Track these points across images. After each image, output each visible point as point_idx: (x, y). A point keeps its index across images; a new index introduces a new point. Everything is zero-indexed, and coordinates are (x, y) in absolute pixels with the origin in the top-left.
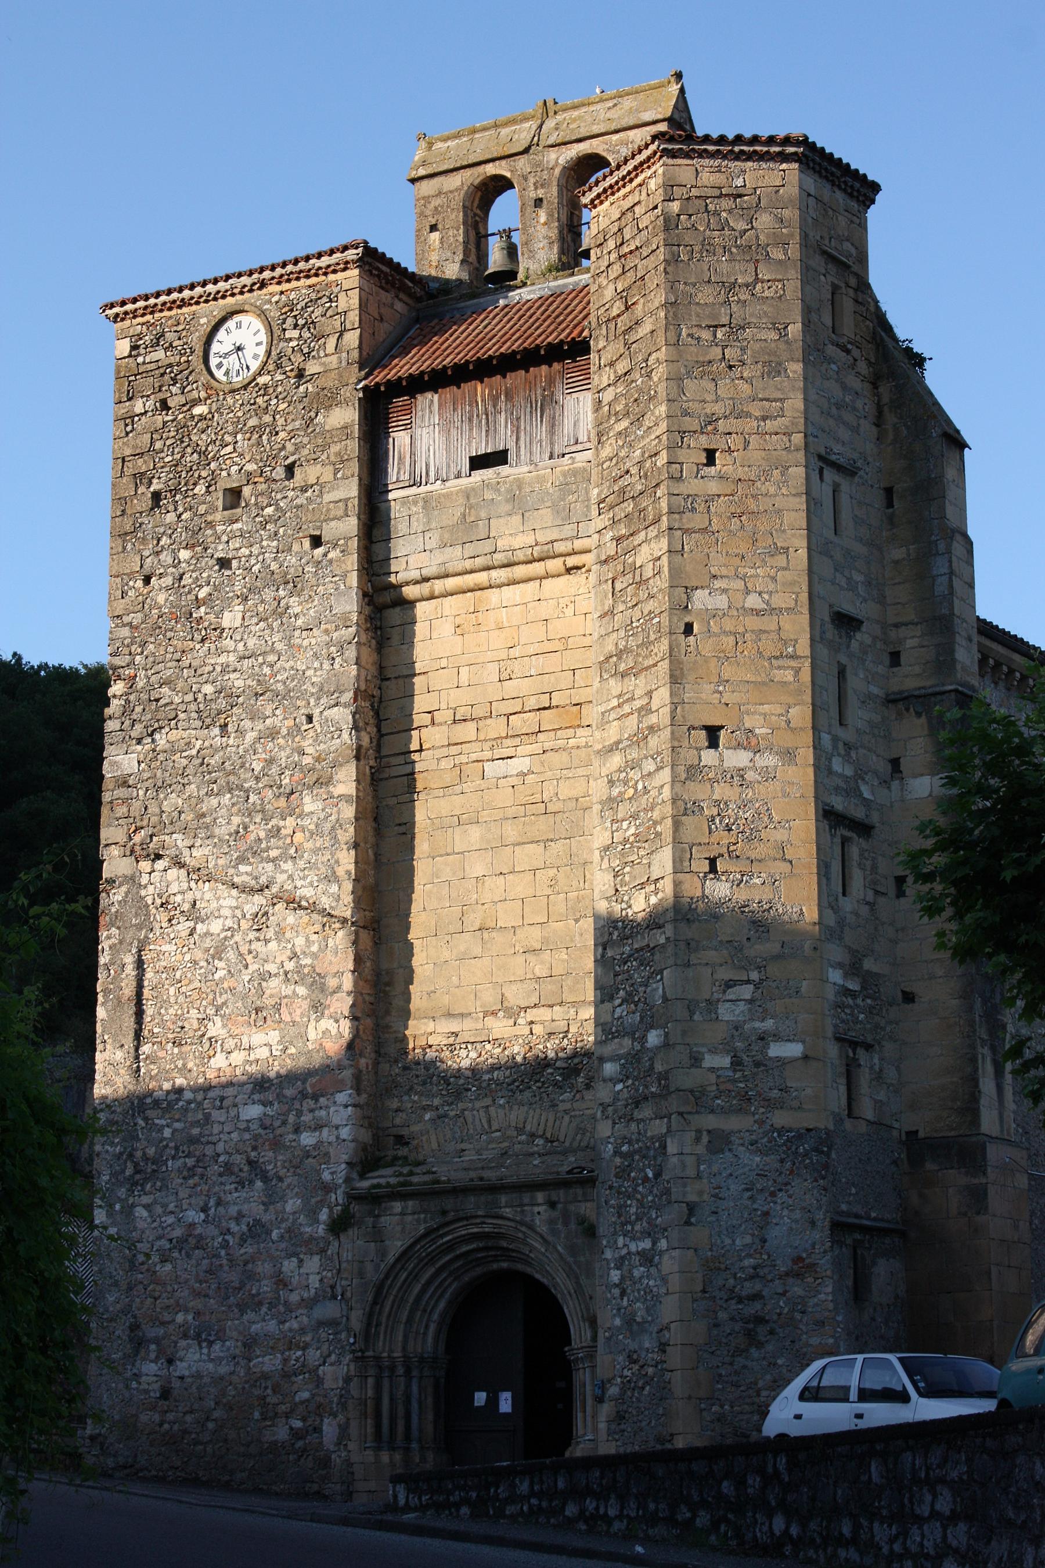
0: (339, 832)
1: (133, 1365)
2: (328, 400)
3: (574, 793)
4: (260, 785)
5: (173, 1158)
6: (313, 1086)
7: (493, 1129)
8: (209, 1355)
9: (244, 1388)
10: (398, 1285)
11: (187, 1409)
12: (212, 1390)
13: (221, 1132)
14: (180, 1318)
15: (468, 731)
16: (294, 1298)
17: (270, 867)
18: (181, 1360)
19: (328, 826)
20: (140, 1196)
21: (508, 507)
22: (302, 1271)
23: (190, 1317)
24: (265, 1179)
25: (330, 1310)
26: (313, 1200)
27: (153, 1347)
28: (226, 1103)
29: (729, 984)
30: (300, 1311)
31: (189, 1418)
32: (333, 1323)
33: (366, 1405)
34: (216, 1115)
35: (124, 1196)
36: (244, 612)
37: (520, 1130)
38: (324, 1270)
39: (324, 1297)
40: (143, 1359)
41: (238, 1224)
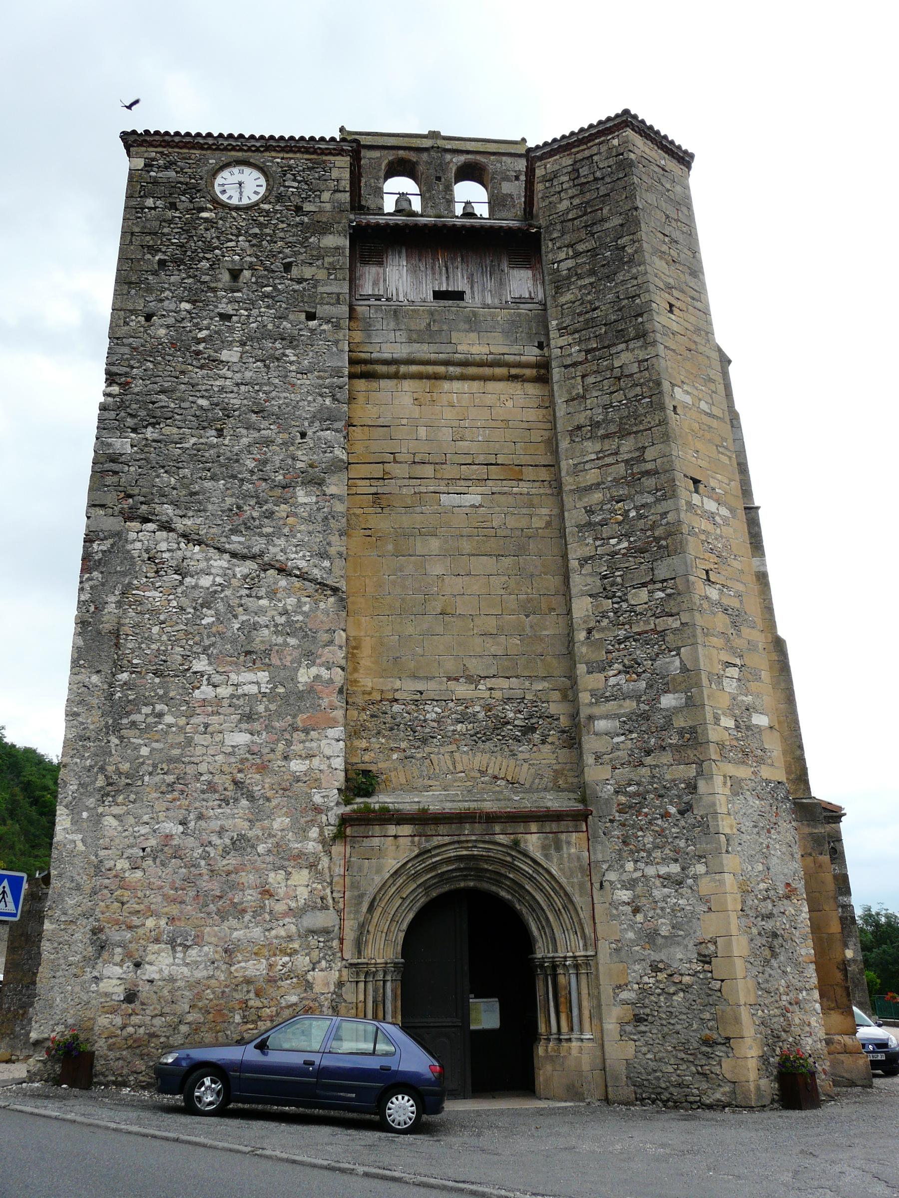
0: (332, 521)
1: (93, 968)
2: (323, 229)
3: (520, 525)
4: (254, 477)
5: (150, 774)
6: (303, 721)
7: (458, 770)
8: (183, 959)
9: (223, 992)
10: (387, 898)
11: (157, 1012)
12: (187, 993)
13: (204, 755)
14: (150, 923)
15: (428, 471)
16: (280, 907)
17: (263, 541)
18: (151, 964)
19: (320, 516)
20: (110, 806)
21: (467, 326)
22: (289, 882)
23: (163, 922)
24: (251, 798)
25: (326, 919)
26: (303, 820)
27: (119, 950)
28: (210, 729)
29: (729, 664)
30: (287, 920)
31: (158, 1021)
32: (326, 931)
34: (198, 739)
35: (92, 806)
36: (243, 353)
37: (483, 773)
38: (314, 882)
39: (314, 908)
40: (105, 962)
41: (221, 838)
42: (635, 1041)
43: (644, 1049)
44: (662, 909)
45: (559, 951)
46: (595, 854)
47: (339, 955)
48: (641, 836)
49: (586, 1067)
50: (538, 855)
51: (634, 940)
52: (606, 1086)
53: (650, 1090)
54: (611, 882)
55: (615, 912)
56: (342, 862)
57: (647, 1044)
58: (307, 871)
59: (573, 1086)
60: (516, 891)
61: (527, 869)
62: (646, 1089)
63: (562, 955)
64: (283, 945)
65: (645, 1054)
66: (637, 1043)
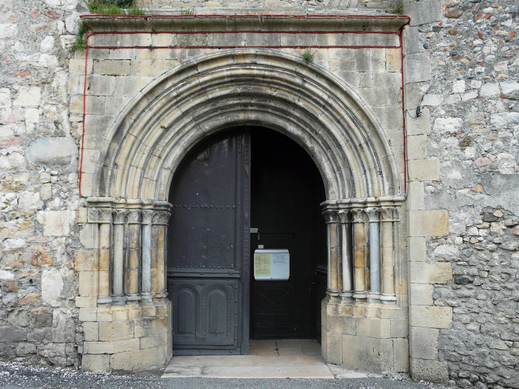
10: (141, 125)
22: (15, 103)
26: (33, 27)
33: (99, 256)
39: (46, 134)
42: (453, 307)
43: (466, 318)
44: (505, 140)
45: (358, 195)
46: (411, 73)
47: (77, 191)
48: (479, 45)
49: (385, 332)
50: (336, 76)
51: (460, 181)
52: (409, 356)
53: (471, 369)
54: (432, 109)
55: (435, 145)
56: (82, 79)
57: (470, 311)
58: (39, 89)
59: (368, 354)
60: (307, 125)
61: (321, 94)
62: (465, 367)
63: (361, 201)
64: (8, 178)
65: (466, 324)
66: (455, 310)
